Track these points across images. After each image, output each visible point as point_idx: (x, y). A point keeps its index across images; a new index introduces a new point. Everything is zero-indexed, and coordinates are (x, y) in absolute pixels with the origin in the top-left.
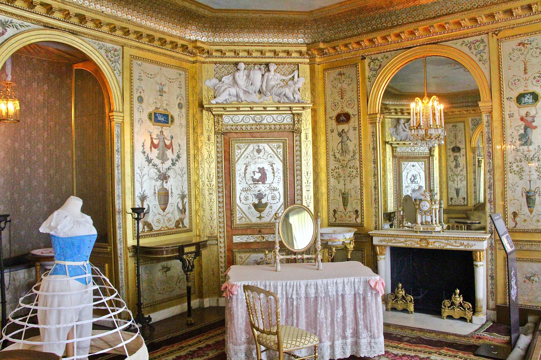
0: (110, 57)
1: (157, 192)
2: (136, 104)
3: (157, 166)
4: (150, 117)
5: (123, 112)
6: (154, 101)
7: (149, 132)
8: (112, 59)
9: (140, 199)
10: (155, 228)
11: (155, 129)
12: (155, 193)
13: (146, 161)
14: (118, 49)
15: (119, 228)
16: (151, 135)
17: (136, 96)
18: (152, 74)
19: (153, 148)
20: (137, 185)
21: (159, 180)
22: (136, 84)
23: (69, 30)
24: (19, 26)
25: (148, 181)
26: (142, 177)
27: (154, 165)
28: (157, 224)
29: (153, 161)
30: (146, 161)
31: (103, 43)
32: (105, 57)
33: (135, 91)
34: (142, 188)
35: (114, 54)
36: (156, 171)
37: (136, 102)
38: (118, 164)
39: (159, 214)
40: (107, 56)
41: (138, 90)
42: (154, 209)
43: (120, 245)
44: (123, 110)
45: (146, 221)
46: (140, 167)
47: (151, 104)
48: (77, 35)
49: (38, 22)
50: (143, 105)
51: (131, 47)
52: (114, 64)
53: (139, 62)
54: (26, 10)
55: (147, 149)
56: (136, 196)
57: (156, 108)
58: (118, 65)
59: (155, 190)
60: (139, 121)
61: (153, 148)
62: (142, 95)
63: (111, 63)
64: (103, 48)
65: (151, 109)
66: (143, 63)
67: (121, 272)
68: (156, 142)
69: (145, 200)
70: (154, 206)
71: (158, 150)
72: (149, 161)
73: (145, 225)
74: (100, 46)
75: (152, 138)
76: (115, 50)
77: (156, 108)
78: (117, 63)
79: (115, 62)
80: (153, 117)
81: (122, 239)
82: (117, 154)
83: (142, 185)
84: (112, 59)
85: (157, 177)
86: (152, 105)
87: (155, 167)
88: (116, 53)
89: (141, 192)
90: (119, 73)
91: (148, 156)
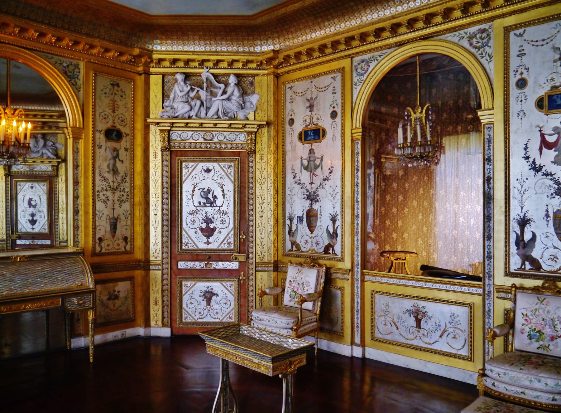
0: (475, 43)
1: (551, 214)
2: (514, 91)
3: (552, 175)
4: (540, 104)
5: (493, 109)
6: (549, 78)
7: (538, 126)
8: (478, 45)
9: (519, 223)
10: (544, 267)
11: (549, 120)
12: (547, 216)
13: (530, 169)
14: (487, 27)
15: (487, 257)
16: (540, 131)
17: (513, 81)
18: (545, 37)
19: (544, 150)
20: (514, 203)
21: (557, 197)
22: (514, 62)
23: (419, 37)
24: (378, 57)
25: (534, 197)
26: (523, 192)
27: (546, 175)
28: (550, 262)
29: (544, 169)
30: (530, 169)
31: (466, 30)
32: (467, 45)
33: (511, 74)
34: (522, 208)
35: (481, 38)
36: (551, 183)
37: (513, 89)
38: (488, 177)
39: (555, 248)
40: (471, 44)
41: (517, 71)
42: (545, 240)
43: (489, 279)
44: (493, 107)
45: (527, 254)
46: (519, 177)
47: (542, 83)
48: (432, 37)
49: (390, 46)
50: (526, 90)
51: (503, 16)
52: (482, 50)
53: (521, 31)
54: (376, 41)
55: (534, 153)
56: (511, 219)
57: (554, 88)
58: (487, 49)
59: (548, 212)
60: (518, 115)
61: (544, 150)
62: (524, 76)
63: (477, 50)
64: (465, 37)
65: (542, 92)
66: (527, 29)
67: (488, 314)
68: (551, 139)
69: (528, 225)
70: (545, 235)
71: (555, 151)
72: (536, 168)
73: (527, 260)
74: (461, 36)
75: (542, 136)
76: (483, 31)
77: (554, 88)
78: (486, 47)
79: (483, 46)
80: (546, 102)
81: (492, 273)
82: (488, 164)
83: (522, 203)
84: (478, 45)
85: (553, 191)
86: (544, 85)
87: (549, 177)
88: (484, 35)
89: (520, 213)
90: (488, 59)
91: (534, 162)
